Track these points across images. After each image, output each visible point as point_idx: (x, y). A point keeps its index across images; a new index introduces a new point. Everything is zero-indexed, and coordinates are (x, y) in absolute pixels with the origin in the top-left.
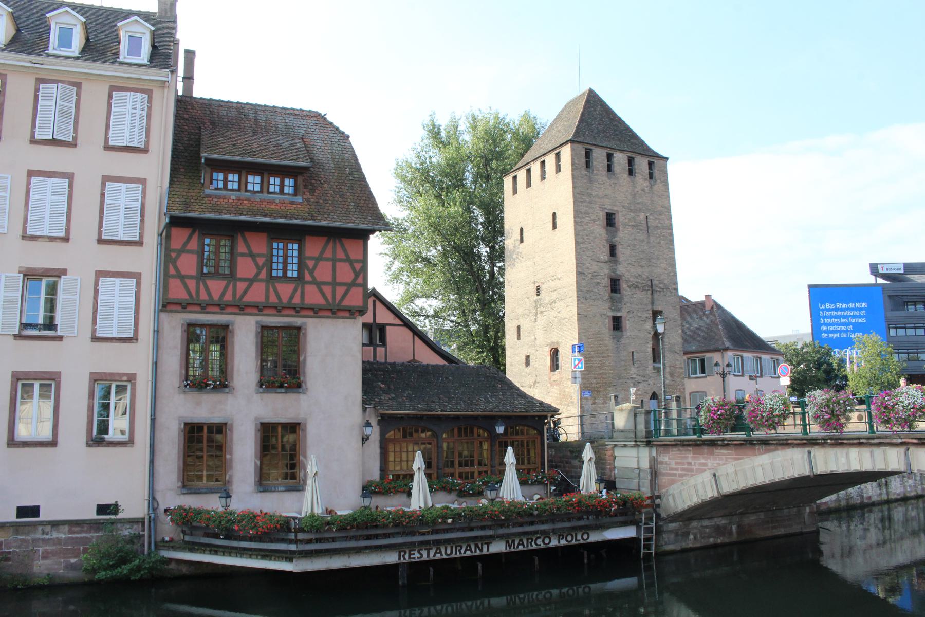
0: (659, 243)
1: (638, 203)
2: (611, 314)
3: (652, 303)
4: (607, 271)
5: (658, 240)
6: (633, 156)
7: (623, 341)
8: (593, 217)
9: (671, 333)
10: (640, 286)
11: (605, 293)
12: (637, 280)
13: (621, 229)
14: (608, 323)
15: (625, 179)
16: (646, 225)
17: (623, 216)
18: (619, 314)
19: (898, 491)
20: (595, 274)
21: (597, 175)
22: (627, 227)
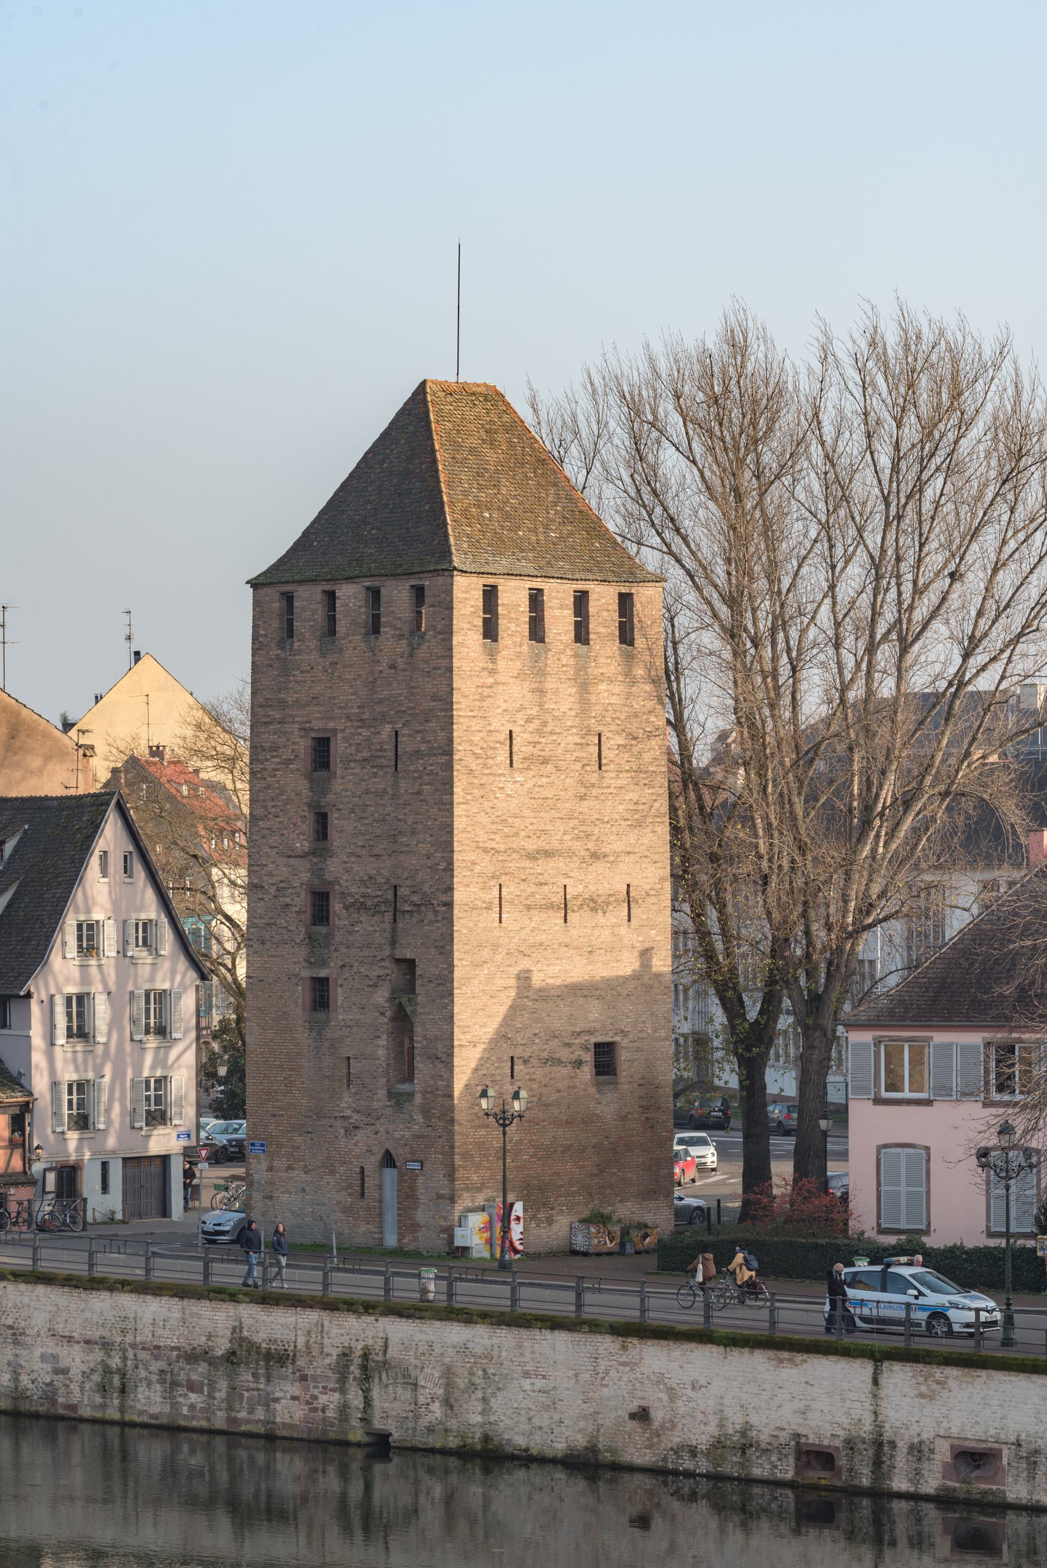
0: (419, 793)
1: (380, 702)
2: (306, 974)
3: (393, 943)
4: (305, 876)
5: (417, 787)
6: (377, 584)
7: (329, 1033)
8: (287, 754)
9: (428, 1013)
10: (369, 903)
11: (296, 925)
12: (363, 890)
13: (339, 772)
14: (301, 994)
15: (355, 649)
16: (391, 754)
17: (346, 739)
18: (323, 973)
19: (155, 1410)
20: (283, 885)
21: (300, 652)
22: (352, 765)
